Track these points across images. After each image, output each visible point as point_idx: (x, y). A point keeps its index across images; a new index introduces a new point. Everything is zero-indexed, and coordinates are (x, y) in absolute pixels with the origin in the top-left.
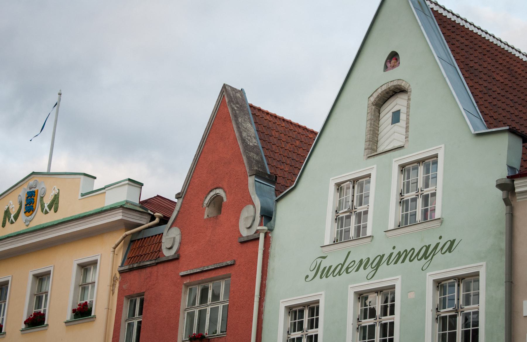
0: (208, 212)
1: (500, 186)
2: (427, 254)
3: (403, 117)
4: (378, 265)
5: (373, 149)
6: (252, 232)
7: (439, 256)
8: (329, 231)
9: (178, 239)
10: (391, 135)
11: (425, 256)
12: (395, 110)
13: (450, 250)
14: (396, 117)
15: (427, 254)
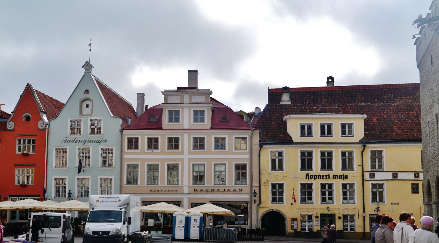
0: (24, 119)
1: (120, 131)
2: (99, 142)
3: (90, 106)
4: (85, 142)
5: (81, 113)
6: (43, 128)
7: (102, 143)
8: (69, 131)
9: (13, 125)
10: (86, 111)
11: (98, 142)
12: (87, 104)
13: (105, 142)
14: (87, 106)
15: (99, 142)
